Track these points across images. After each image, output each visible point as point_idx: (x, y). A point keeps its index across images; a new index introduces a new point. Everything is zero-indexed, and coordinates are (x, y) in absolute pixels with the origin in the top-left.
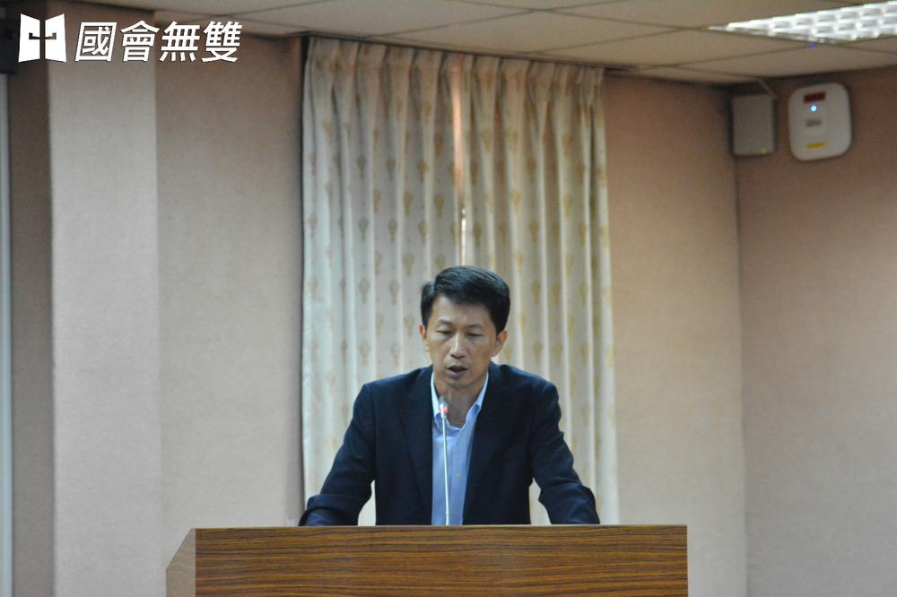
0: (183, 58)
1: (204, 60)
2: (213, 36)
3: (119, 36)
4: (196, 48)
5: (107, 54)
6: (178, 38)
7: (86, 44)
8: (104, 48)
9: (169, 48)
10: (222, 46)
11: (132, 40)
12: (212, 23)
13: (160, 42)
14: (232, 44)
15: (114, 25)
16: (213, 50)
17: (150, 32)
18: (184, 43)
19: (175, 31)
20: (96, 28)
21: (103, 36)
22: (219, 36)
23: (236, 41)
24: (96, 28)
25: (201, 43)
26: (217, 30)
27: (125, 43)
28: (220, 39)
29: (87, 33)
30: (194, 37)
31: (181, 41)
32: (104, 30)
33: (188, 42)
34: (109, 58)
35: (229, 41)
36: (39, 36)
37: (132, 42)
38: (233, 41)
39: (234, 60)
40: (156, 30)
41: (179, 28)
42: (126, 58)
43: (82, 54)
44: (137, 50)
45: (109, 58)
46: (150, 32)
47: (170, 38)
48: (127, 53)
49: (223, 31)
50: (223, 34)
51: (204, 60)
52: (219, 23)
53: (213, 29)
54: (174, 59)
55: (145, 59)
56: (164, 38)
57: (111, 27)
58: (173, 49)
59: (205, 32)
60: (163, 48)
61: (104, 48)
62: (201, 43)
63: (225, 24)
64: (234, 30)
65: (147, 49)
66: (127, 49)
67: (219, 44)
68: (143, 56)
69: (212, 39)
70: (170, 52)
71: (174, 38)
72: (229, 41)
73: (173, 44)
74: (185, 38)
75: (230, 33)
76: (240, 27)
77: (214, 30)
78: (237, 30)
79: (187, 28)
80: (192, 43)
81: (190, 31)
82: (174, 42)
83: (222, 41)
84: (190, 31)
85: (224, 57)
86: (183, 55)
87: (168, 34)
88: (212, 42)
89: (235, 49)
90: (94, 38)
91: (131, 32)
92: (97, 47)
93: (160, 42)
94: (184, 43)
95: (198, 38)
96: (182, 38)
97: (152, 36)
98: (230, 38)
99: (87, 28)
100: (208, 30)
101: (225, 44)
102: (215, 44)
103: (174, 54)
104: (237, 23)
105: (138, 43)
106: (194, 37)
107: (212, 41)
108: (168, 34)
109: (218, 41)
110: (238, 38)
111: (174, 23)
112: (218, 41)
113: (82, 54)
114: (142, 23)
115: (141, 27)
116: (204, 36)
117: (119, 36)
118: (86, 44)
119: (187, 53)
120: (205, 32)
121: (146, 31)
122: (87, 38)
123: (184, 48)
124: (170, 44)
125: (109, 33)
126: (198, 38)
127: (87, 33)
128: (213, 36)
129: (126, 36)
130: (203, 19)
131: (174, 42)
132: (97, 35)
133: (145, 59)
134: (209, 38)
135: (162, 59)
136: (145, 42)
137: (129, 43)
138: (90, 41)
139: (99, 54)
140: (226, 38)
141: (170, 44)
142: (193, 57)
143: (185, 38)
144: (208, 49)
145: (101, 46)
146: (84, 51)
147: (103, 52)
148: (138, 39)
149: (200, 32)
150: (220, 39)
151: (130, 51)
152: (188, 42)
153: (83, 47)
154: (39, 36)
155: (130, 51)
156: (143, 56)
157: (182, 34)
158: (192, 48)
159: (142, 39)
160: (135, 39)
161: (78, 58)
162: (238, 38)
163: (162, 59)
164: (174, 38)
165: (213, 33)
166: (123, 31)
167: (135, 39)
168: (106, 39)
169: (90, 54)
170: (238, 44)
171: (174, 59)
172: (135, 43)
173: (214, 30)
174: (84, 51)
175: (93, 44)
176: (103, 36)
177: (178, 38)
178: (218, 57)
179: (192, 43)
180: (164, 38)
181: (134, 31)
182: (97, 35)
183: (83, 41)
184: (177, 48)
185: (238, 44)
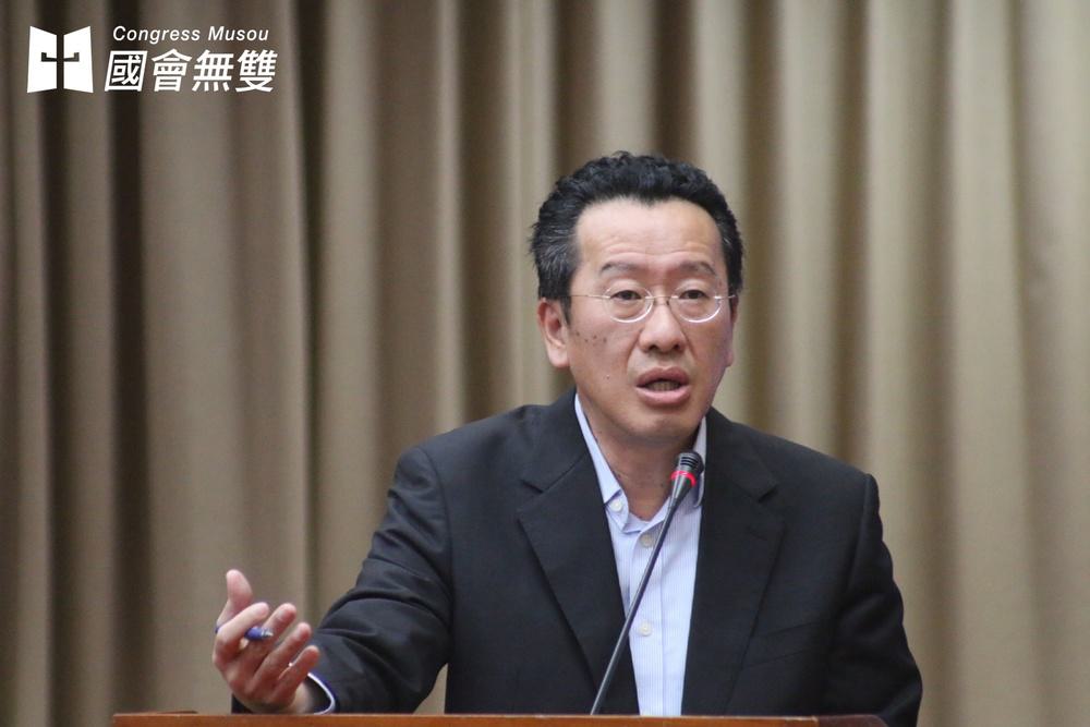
0: (216, 88)
1: (238, 90)
2: (247, 65)
3: (150, 66)
4: (230, 78)
6: (211, 67)
7: (116, 73)
9: (202, 77)
10: (256, 76)
11: (163, 69)
12: (246, 51)
13: (192, 71)
14: (267, 73)
16: (247, 80)
17: (181, 61)
18: (218, 72)
19: (208, 60)
20: (126, 57)
22: (254, 65)
23: (271, 71)
24: (126, 57)
25: (235, 73)
26: (251, 59)
27: (156, 72)
29: (116, 61)
30: (228, 67)
32: (134, 58)
33: (222, 71)
34: (139, 88)
35: (264, 70)
36: (65, 63)
37: (163, 72)
38: (267, 70)
39: (269, 90)
40: (188, 59)
41: (213, 56)
42: (157, 88)
44: (168, 80)
46: (181, 61)
47: (203, 67)
48: (158, 83)
51: (238, 90)
52: (254, 52)
54: (207, 88)
55: (177, 89)
56: (197, 67)
57: (141, 56)
59: (239, 60)
60: (196, 78)
62: (235, 73)
63: (259, 52)
65: (179, 79)
66: (158, 79)
67: (254, 74)
70: (203, 82)
71: (207, 67)
72: (264, 70)
73: (206, 74)
74: (219, 67)
75: (265, 61)
76: (276, 56)
77: (248, 59)
79: (220, 57)
80: (225, 73)
81: (223, 60)
82: (207, 71)
83: (256, 71)
84: (223, 60)
85: (259, 87)
87: (201, 63)
89: (270, 79)
90: (124, 68)
91: (162, 61)
92: (126, 76)
94: (218, 72)
95: (232, 67)
96: (215, 67)
97: (185, 66)
99: (116, 57)
100: (242, 59)
101: (260, 73)
102: (249, 73)
103: (207, 85)
104: (272, 52)
105: (170, 72)
107: (246, 71)
108: (201, 63)
110: (273, 67)
111: (207, 51)
113: (111, 84)
114: (174, 51)
116: (238, 66)
117: (150, 66)
118: (116, 73)
119: (221, 83)
120: (239, 60)
122: (117, 68)
123: (217, 77)
124: (202, 73)
125: (138, 61)
126: (232, 67)
127: (116, 61)
128: (247, 65)
129: (157, 65)
130: (236, 48)
131: (207, 71)
132: (126, 64)
133: (177, 89)
134: (243, 68)
135: (195, 89)
136: (176, 72)
137: (160, 73)
138: (120, 70)
139: (129, 84)
140: (261, 67)
141: (202, 73)
142: (226, 87)
143: (219, 67)
144: (242, 79)
145: (131, 75)
146: (114, 80)
147: (134, 82)
148: (170, 69)
149: (231, 61)
152: (222, 71)
153: (112, 77)
154: (65, 63)
157: (215, 63)
158: (226, 77)
160: (166, 68)
161: (108, 88)
162: (273, 67)
163: (195, 89)
164: (207, 67)
166: (154, 59)
167: (166, 68)
169: (119, 84)
170: (273, 74)
171: (207, 88)
172: (166, 73)
173: (248, 59)
174: (114, 80)
175: (123, 73)
176: (133, 65)
177: (211, 67)
178: (253, 87)
179: (225, 73)
180: (197, 67)
182: (126, 64)
184: (210, 77)
185: (273, 74)
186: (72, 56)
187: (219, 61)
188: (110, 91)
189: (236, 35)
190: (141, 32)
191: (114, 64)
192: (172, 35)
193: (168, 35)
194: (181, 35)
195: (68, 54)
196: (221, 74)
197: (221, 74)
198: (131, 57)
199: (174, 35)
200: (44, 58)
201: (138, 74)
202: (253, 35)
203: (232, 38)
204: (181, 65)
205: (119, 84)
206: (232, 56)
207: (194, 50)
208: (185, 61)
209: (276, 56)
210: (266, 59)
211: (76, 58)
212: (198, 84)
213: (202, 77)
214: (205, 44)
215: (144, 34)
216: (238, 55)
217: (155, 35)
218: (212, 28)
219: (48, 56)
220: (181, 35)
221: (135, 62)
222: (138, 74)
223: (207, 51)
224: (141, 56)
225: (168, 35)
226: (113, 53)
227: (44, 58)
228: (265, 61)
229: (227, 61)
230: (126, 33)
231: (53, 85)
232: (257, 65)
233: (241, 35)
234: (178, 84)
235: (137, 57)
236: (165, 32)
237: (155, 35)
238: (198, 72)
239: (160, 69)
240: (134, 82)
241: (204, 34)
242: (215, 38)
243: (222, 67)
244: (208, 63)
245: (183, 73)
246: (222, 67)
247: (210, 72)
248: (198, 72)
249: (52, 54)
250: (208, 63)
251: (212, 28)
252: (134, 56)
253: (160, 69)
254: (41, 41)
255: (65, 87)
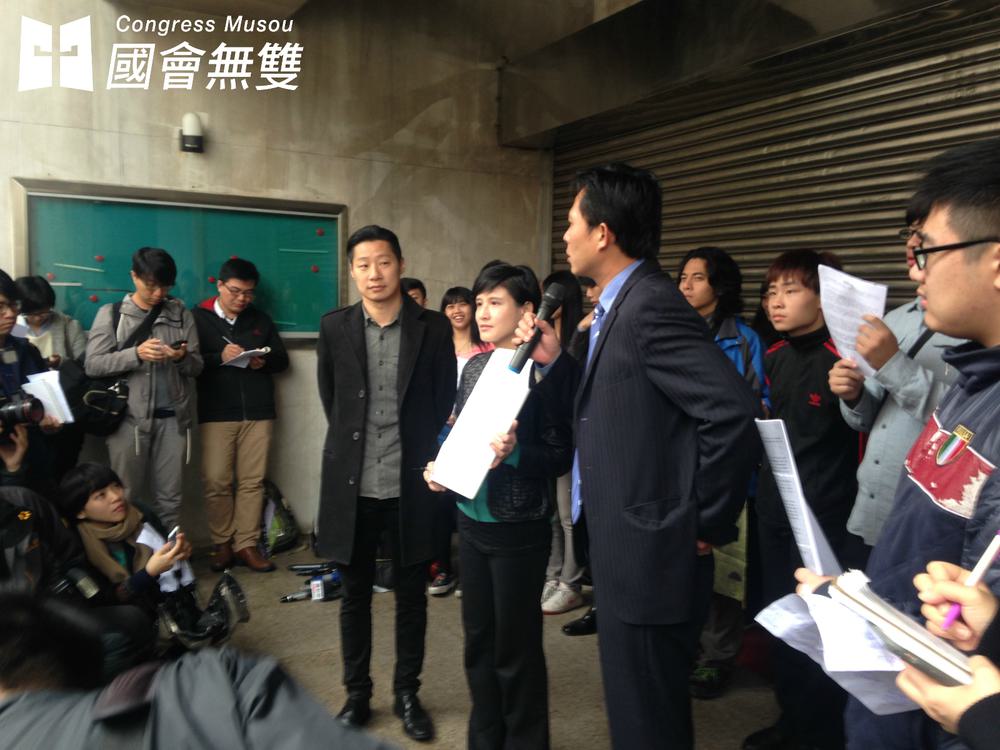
0: (233, 85)
1: (259, 88)
2: (268, 60)
3: (159, 59)
4: (249, 75)
5: (143, 82)
6: (228, 62)
7: (119, 69)
8: (140, 74)
9: (217, 74)
10: (279, 72)
11: (173, 64)
12: (268, 44)
13: (206, 67)
14: (292, 69)
15: (152, 46)
16: (269, 77)
17: (194, 55)
18: (235, 68)
19: (225, 54)
20: (131, 51)
21: (139, 60)
22: (276, 60)
23: (296, 66)
24: (131, 51)
25: (255, 68)
27: (165, 68)
28: (277, 63)
30: (246, 62)
31: (231, 66)
33: (240, 67)
35: (288, 66)
36: (62, 58)
37: (173, 67)
38: (292, 66)
39: (293, 88)
40: (202, 52)
41: (229, 50)
42: (166, 86)
43: (114, 81)
44: (179, 76)
45: (146, 86)
46: (194, 55)
47: (218, 62)
49: (280, 54)
50: (281, 57)
51: (259, 88)
52: (276, 45)
53: (268, 51)
54: (223, 86)
55: (189, 87)
56: (211, 62)
57: (148, 50)
58: (222, 75)
59: (260, 55)
60: (210, 75)
61: (140, 74)
62: (255, 68)
63: (282, 45)
64: (294, 52)
65: (191, 76)
66: (168, 75)
67: (277, 70)
68: (186, 83)
69: (268, 63)
70: (218, 79)
71: (223, 62)
72: (288, 66)
73: (222, 70)
74: (236, 62)
75: (289, 56)
76: (301, 49)
77: (270, 52)
78: (298, 52)
79: (238, 50)
80: (244, 68)
81: (242, 54)
82: (223, 66)
83: (279, 66)
84: (242, 54)
86: (233, 82)
87: (216, 58)
88: (268, 66)
89: (295, 76)
90: (128, 63)
91: (171, 55)
93: (206, 67)
94: (235, 68)
95: (251, 62)
96: (232, 62)
97: (197, 60)
98: (288, 63)
99: (120, 51)
100: (263, 53)
101: (283, 69)
102: (271, 69)
103: (222, 81)
104: (297, 45)
105: (181, 67)
106: (246, 62)
107: (267, 66)
108: (216, 58)
109: (275, 66)
110: (298, 63)
111: (223, 44)
112: (275, 66)
113: (114, 81)
114: (185, 44)
115: (184, 49)
116: (258, 61)
117: (159, 59)
118: (119, 69)
119: (238, 80)
120: (260, 55)
121: (190, 54)
123: (235, 74)
124: (218, 68)
125: (146, 56)
126: (251, 62)
127: (120, 56)
128: (268, 60)
129: (166, 60)
130: (257, 41)
131: (223, 66)
132: (131, 59)
134: (264, 63)
135: (209, 86)
136: (188, 67)
137: (170, 69)
138: (124, 66)
139: (134, 81)
140: (285, 62)
141: (218, 68)
143: (236, 62)
144: (263, 76)
145: (136, 71)
146: (117, 77)
147: (140, 79)
148: (181, 64)
150: (278, 56)
151: (171, 78)
152: (240, 67)
153: (115, 73)
155: (171, 78)
156: (186, 83)
157: (233, 57)
158: (244, 74)
159: (185, 64)
160: (177, 64)
161: (110, 86)
162: (298, 63)
163: (209, 86)
164: (223, 62)
165: (269, 56)
166: (163, 53)
167: (177, 64)
168: (143, 63)
169: (123, 81)
170: (298, 70)
171: (223, 86)
173: (270, 52)
174: (117, 77)
175: (127, 69)
176: (139, 60)
177: (228, 62)
178: (275, 85)
179: (244, 68)
180: (211, 62)
181: (175, 54)
182: (131, 59)
183: (131, 65)
184: (226, 74)
185: (298, 70)
186: (70, 50)
187: (237, 56)
188: (112, 89)
189: (256, 26)
190: (148, 22)
191: (117, 59)
192: (183, 25)
193: (178, 25)
194: (193, 25)
195: (65, 47)
196: (239, 70)
197: (239, 70)
198: (136, 51)
199: (185, 25)
200: (38, 51)
201: (144, 70)
202: (275, 26)
203: (252, 29)
204: (193, 59)
205: (123, 81)
206: (251, 49)
207: (207, 42)
208: (197, 56)
209: (301, 49)
210: (290, 52)
211: (74, 51)
212: (213, 81)
213: (217, 74)
214: (222, 36)
215: (151, 24)
216: (258, 48)
217: (164, 26)
218: (229, 18)
219: (42, 50)
220: (193, 25)
221: (141, 56)
222: (144, 70)
223: (223, 44)
224: (148, 50)
225: (178, 25)
226: (116, 46)
227: (38, 51)
228: (289, 56)
229: (246, 55)
230: (130, 24)
231: (50, 85)
232: (280, 60)
233: (262, 26)
234: (190, 81)
235: (144, 51)
236: (175, 23)
237: (164, 26)
238: (213, 68)
239: (169, 64)
240: (140, 79)
241: (220, 24)
242: (232, 29)
243: (240, 62)
244: (224, 57)
245: (196, 68)
246: (240, 62)
247: (227, 68)
248: (213, 68)
249: (47, 47)
250: (224, 57)
251: (229, 18)
252: (140, 49)
253: (169, 64)
254: (35, 32)
255: (62, 85)
